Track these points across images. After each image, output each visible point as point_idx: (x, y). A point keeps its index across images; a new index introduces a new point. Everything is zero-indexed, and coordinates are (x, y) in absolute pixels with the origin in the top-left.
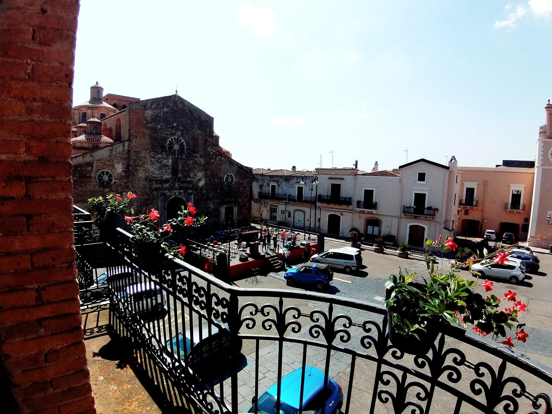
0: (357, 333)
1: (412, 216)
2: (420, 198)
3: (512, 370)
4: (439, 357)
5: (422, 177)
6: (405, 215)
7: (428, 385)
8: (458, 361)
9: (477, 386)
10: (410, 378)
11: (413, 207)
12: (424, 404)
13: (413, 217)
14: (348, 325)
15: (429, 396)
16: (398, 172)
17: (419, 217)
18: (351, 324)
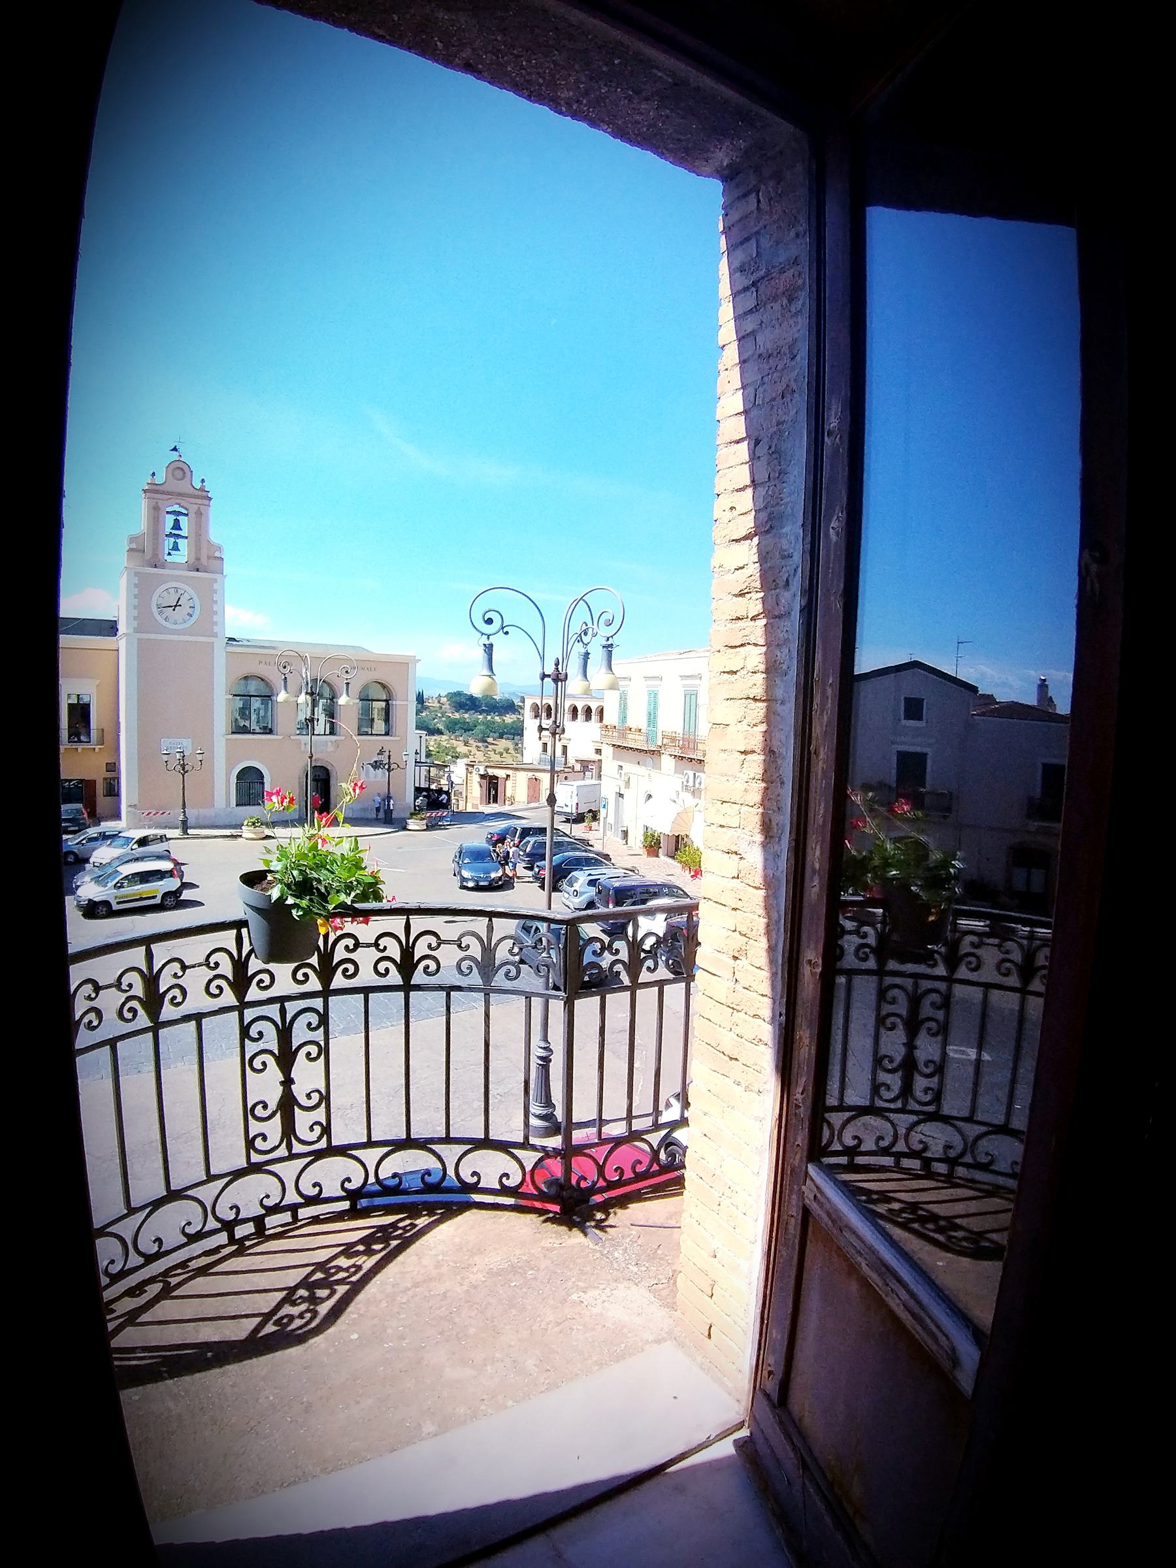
0: (195, 980)
3: (419, 924)
4: (326, 957)
7: (318, 1003)
8: (351, 947)
10: (292, 1008)
12: (319, 1035)
14: (180, 974)
15: (324, 1020)
18: (184, 967)
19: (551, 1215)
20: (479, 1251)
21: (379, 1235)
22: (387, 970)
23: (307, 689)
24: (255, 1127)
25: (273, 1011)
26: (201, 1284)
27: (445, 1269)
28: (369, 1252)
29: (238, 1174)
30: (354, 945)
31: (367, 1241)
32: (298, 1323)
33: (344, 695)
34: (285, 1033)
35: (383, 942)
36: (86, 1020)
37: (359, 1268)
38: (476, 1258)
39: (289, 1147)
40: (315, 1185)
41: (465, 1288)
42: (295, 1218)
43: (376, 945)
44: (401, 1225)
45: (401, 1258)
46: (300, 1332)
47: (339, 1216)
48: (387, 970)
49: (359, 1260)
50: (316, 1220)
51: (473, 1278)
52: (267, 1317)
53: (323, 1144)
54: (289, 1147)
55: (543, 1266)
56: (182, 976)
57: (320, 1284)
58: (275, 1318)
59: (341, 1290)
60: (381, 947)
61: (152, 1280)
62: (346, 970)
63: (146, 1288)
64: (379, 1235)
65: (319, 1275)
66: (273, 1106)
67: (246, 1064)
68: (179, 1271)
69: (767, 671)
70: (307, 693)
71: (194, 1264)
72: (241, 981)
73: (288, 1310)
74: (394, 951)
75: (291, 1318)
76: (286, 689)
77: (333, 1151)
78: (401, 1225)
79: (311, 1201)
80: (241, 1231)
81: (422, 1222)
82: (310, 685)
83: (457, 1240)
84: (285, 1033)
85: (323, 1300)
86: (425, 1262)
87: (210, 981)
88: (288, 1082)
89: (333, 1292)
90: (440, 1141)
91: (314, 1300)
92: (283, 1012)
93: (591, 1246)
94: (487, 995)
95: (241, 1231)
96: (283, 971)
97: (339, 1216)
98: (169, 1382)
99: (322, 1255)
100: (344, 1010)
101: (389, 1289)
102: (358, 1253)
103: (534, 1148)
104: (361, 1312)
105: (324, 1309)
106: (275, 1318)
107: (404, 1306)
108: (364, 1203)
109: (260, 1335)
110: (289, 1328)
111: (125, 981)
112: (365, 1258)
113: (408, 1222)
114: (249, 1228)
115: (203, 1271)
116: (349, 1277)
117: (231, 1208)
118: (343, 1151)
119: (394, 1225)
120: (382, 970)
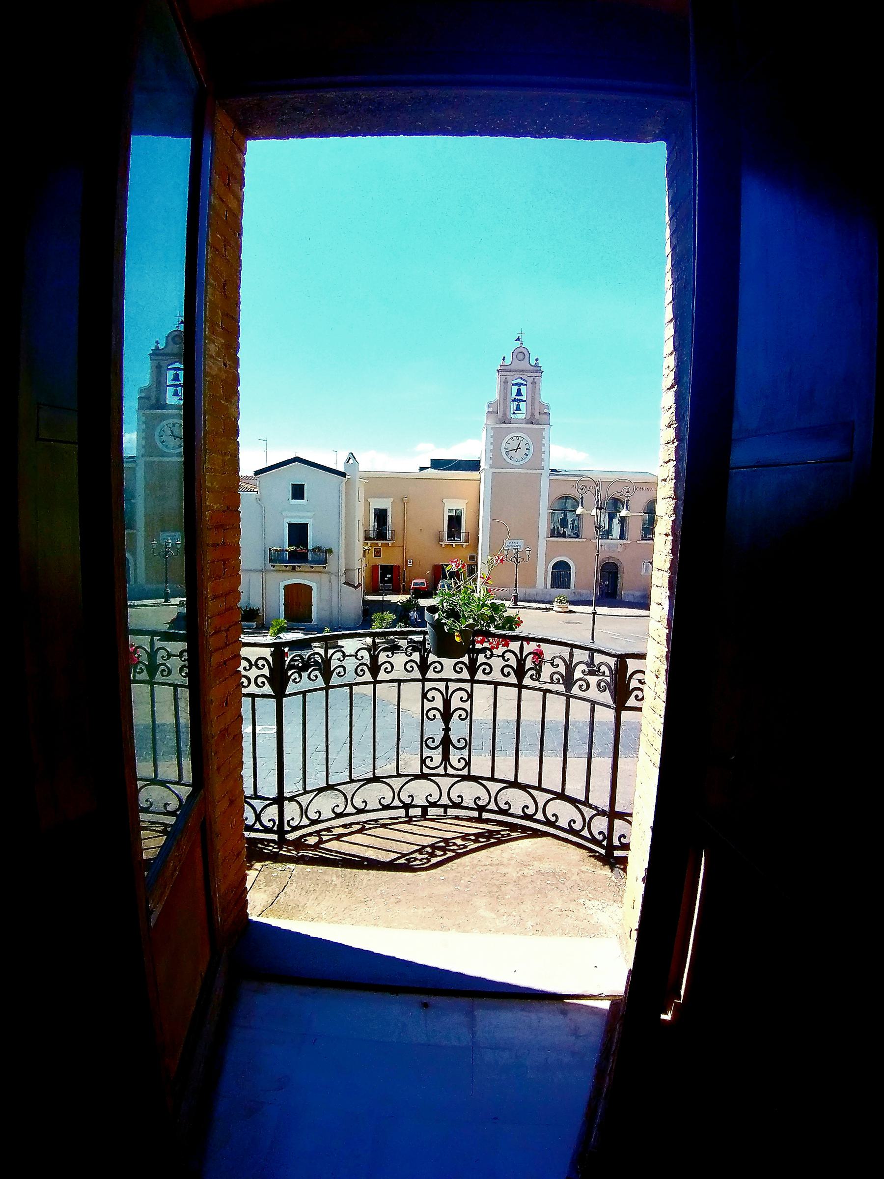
1: (287, 566)
2: (298, 532)
5: (298, 492)
6: (274, 566)
7: (467, 686)
9: (506, 670)
11: (287, 551)
12: (467, 706)
13: (289, 568)
15: (470, 696)
16: (253, 482)
17: (299, 567)
19: (597, 854)
20: (541, 860)
21: (486, 834)
22: (509, 673)
23: (598, 505)
24: (427, 753)
25: (441, 686)
26: (381, 832)
27: (513, 862)
28: (475, 841)
29: (416, 777)
30: (490, 655)
31: (478, 835)
32: (418, 862)
33: (580, 507)
34: (447, 702)
35: (507, 655)
36: (337, 670)
37: (465, 847)
38: (535, 863)
39: (446, 769)
40: (459, 796)
41: (518, 875)
42: (445, 812)
43: (503, 656)
44: (502, 833)
45: (492, 849)
46: (415, 867)
47: (470, 819)
48: (509, 673)
49: (467, 843)
50: (457, 818)
51: (526, 871)
52: (404, 855)
53: (465, 772)
54: (446, 769)
55: (573, 878)
56: (392, 657)
57: (440, 848)
58: (407, 857)
59: (450, 854)
60: (506, 658)
61: (358, 823)
62: (485, 669)
63: (352, 826)
64: (486, 834)
65: (442, 844)
66: (437, 743)
67: (424, 714)
68: (373, 823)
69: (675, 478)
70: (597, 508)
71: (381, 822)
72: (424, 667)
73: (416, 855)
74: (513, 662)
75: (416, 859)
76: (582, 506)
77: (469, 778)
78: (502, 833)
79: (456, 806)
80: (413, 812)
81: (514, 835)
82: (600, 503)
83: (530, 850)
84: (447, 702)
85: (437, 856)
86: (504, 855)
87: (407, 663)
88: (447, 730)
89: (445, 854)
90: (534, 788)
91: (432, 855)
92: (447, 688)
93: (613, 878)
94: (568, 698)
95: (413, 812)
96: (448, 663)
97: (470, 819)
98: (340, 869)
99: (449, 835)
100: (483, 693)
101: (475, 862)
102: (470, 840)
103: (590, 806)
104: (453, 868)
105: (434, 860)
106: (407, 857)
107: (478, 872)
108: (485, 815)
109: (395, 862)
110: (412, 864)
111: (360, 654)
112: (472, 843)
113: (507, 832)
114: (417, 812)
115: (384, 826)
116: (457, 850)
117: (409, 796)
118: (476, 779)
119: (498, 832)
120: (506, 672)
